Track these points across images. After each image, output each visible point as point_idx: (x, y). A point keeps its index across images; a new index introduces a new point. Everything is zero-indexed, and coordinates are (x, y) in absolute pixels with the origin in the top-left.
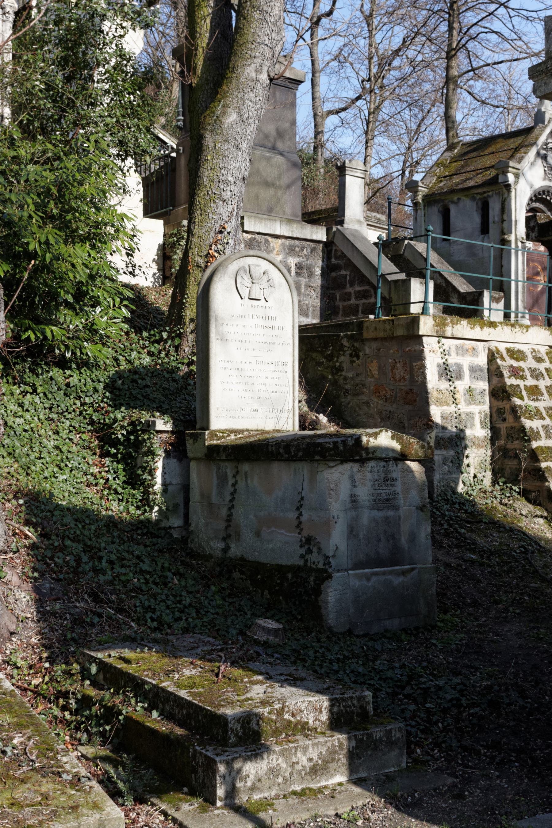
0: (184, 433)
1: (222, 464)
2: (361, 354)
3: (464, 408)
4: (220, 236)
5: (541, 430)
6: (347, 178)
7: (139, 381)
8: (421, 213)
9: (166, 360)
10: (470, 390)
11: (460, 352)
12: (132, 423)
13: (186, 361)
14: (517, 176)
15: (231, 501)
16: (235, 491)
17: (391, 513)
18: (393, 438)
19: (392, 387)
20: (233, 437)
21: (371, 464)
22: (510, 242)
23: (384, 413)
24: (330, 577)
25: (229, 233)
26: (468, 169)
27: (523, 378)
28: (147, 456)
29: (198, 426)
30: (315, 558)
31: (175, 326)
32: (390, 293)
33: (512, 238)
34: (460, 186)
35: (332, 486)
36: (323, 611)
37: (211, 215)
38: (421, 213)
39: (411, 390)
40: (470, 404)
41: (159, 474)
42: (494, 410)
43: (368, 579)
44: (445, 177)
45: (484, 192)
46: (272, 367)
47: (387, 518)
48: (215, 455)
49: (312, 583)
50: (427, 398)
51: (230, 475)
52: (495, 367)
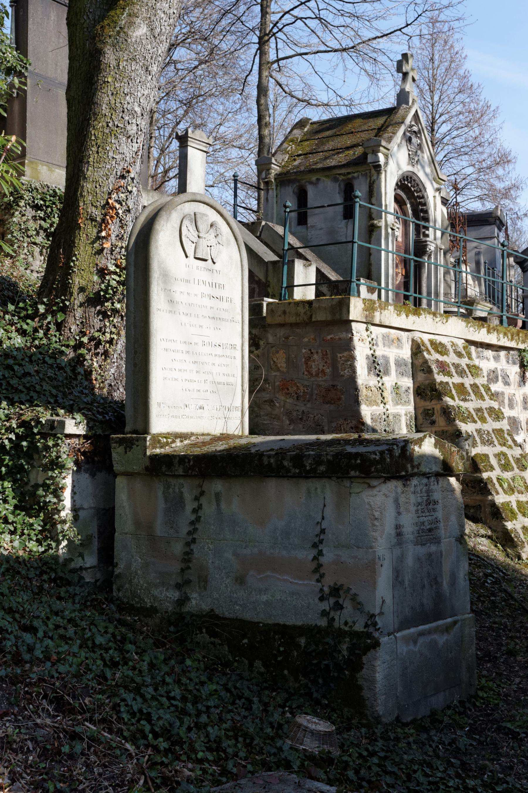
0: (107, 438)
1: (173, 481)
2: (261, 343)
3: (392, 409)
4: (122, 182)
5: (475, 434)
6: (190, 149)
7: (16, 368)
8: (272, 193)
9: (45, 341)
10: (396, 387)
11: (386, 342)
12: (23, 424)
13: (72, 343)
14: (386, 157)
15: (189, 533)
16: (198, 519)
17: (433, 548)
18: (436, 446)
19: (306, 383)
20: (178, 443)
22: (380, 227)
23: (295, 413)
24: (376, 644)
25: (133, 179)
26: (326, 148)
27: (450, 375)
28: (53, 470)
29: (128, 428)
30: (347, 617)
31: (57, 297)
32: (267, 276)
33: (382, 224)
34: (320, 166)
35: (377, 514)
36: (366, 693)
37: (111, 154)
38: (272, 193)
39: (334, 386)
40: (397, 404)
41: (67, 495)
42: (420, 411)
43: (415, 642)
44: (299, 156)
45: (349, 173)
46: (219, 351)
47: (430, 555)
48: (164, 469)
49: (345, 653)
50: (357, 396)
51: (188, 497)
52: (421, 361)
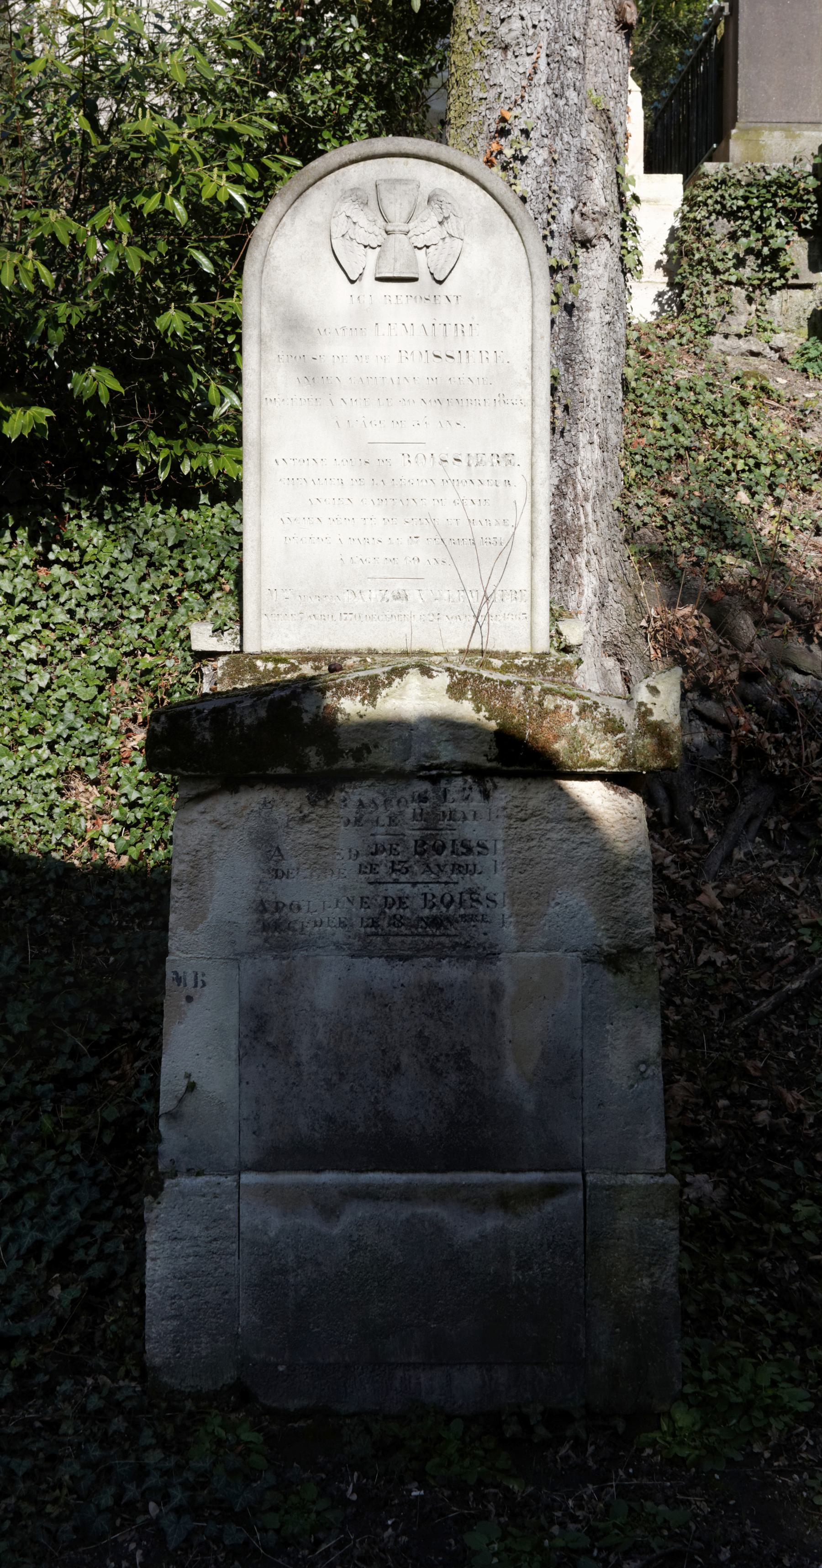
17: (451, 972)
21: (359, 793)
43: (329, 1211)
47: (432, 991)
